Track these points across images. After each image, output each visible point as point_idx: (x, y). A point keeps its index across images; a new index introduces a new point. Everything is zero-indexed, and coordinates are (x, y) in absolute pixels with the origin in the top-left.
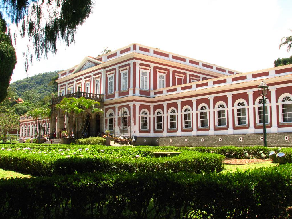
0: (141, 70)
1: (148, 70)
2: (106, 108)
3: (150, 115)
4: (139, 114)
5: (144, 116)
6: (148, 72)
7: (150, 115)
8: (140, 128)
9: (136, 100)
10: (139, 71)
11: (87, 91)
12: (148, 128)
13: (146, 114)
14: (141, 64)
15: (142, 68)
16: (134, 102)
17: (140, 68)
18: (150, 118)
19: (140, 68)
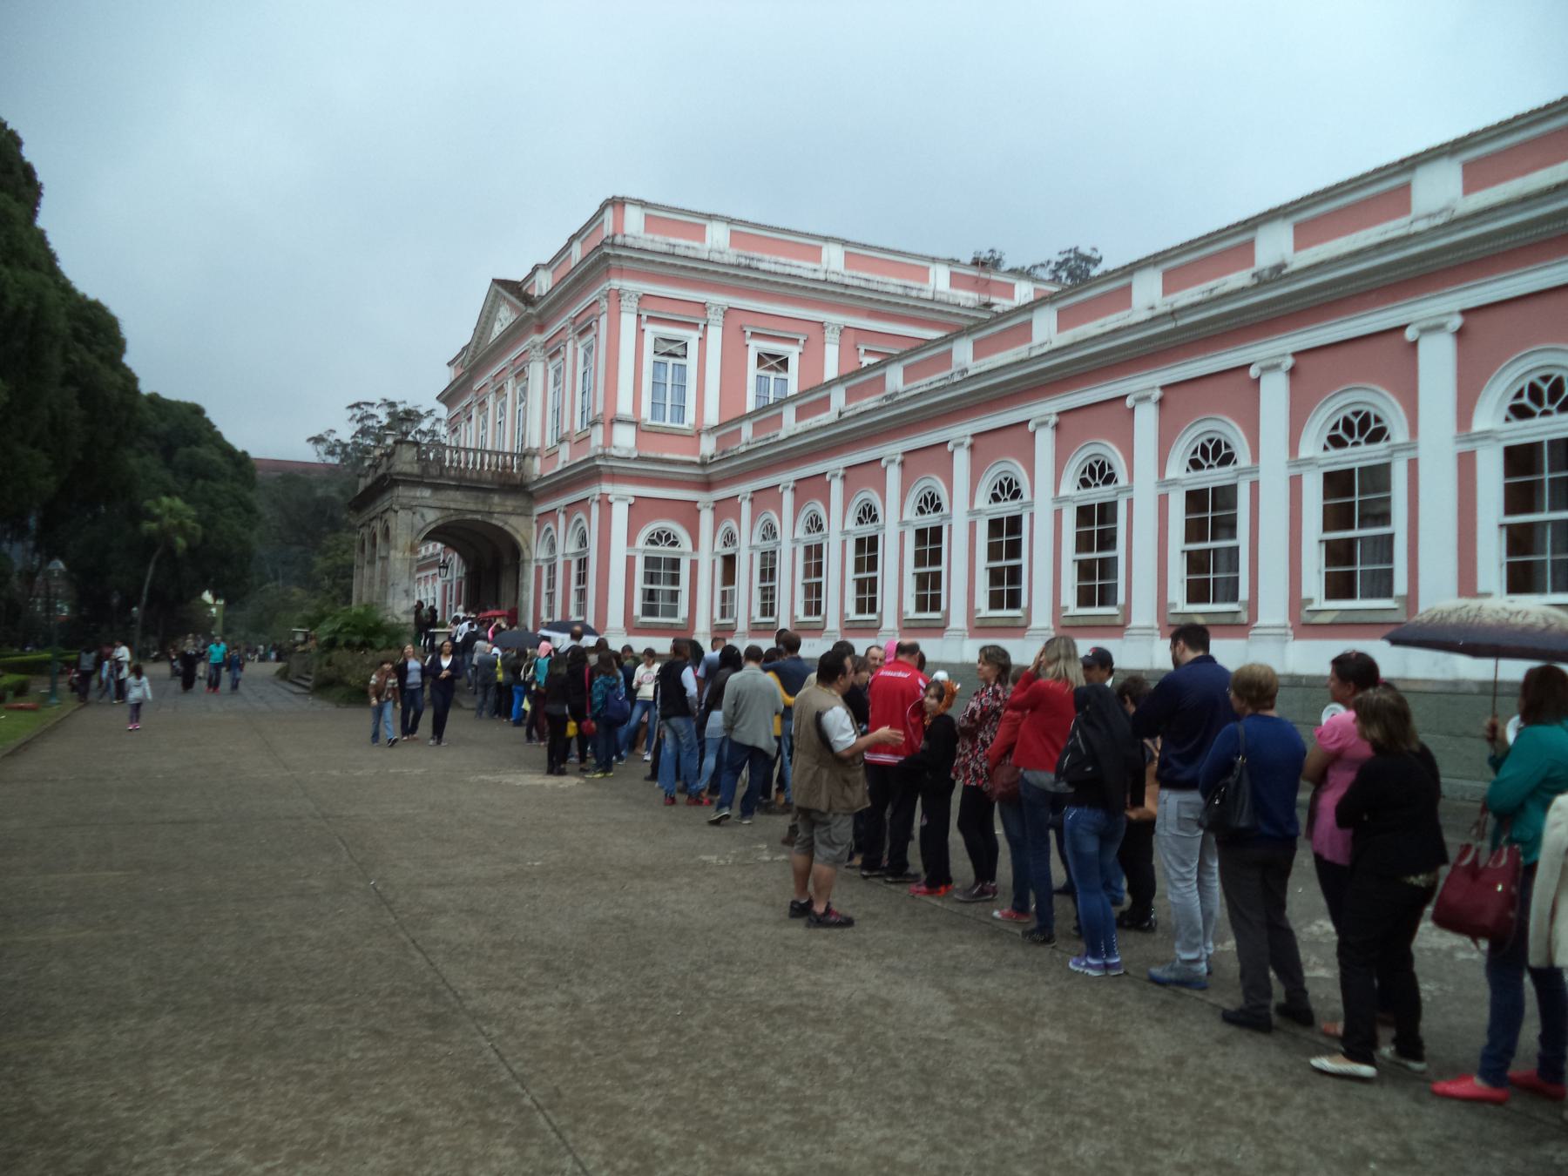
0: (652, 330)
1: (696, 325)
2: (539, 515)
3: (695, 546)
4: (631, 540)
5: (663, 550)
6: (692, 337)
7: (695, 546)
8: (637, 609)
9: (615, 477)
10: (640, 332)
11: (465, 443)
12: (683, 611)
13: (674, 544)
14: (644, 298)
15: (651, 319)
16: (606, 488)
17: (644, 318)
18: (694, 565)
19: (644, 318)
